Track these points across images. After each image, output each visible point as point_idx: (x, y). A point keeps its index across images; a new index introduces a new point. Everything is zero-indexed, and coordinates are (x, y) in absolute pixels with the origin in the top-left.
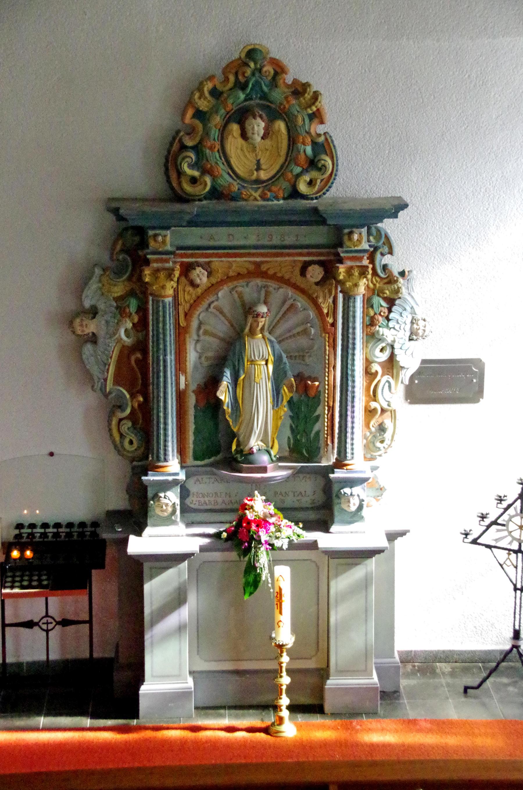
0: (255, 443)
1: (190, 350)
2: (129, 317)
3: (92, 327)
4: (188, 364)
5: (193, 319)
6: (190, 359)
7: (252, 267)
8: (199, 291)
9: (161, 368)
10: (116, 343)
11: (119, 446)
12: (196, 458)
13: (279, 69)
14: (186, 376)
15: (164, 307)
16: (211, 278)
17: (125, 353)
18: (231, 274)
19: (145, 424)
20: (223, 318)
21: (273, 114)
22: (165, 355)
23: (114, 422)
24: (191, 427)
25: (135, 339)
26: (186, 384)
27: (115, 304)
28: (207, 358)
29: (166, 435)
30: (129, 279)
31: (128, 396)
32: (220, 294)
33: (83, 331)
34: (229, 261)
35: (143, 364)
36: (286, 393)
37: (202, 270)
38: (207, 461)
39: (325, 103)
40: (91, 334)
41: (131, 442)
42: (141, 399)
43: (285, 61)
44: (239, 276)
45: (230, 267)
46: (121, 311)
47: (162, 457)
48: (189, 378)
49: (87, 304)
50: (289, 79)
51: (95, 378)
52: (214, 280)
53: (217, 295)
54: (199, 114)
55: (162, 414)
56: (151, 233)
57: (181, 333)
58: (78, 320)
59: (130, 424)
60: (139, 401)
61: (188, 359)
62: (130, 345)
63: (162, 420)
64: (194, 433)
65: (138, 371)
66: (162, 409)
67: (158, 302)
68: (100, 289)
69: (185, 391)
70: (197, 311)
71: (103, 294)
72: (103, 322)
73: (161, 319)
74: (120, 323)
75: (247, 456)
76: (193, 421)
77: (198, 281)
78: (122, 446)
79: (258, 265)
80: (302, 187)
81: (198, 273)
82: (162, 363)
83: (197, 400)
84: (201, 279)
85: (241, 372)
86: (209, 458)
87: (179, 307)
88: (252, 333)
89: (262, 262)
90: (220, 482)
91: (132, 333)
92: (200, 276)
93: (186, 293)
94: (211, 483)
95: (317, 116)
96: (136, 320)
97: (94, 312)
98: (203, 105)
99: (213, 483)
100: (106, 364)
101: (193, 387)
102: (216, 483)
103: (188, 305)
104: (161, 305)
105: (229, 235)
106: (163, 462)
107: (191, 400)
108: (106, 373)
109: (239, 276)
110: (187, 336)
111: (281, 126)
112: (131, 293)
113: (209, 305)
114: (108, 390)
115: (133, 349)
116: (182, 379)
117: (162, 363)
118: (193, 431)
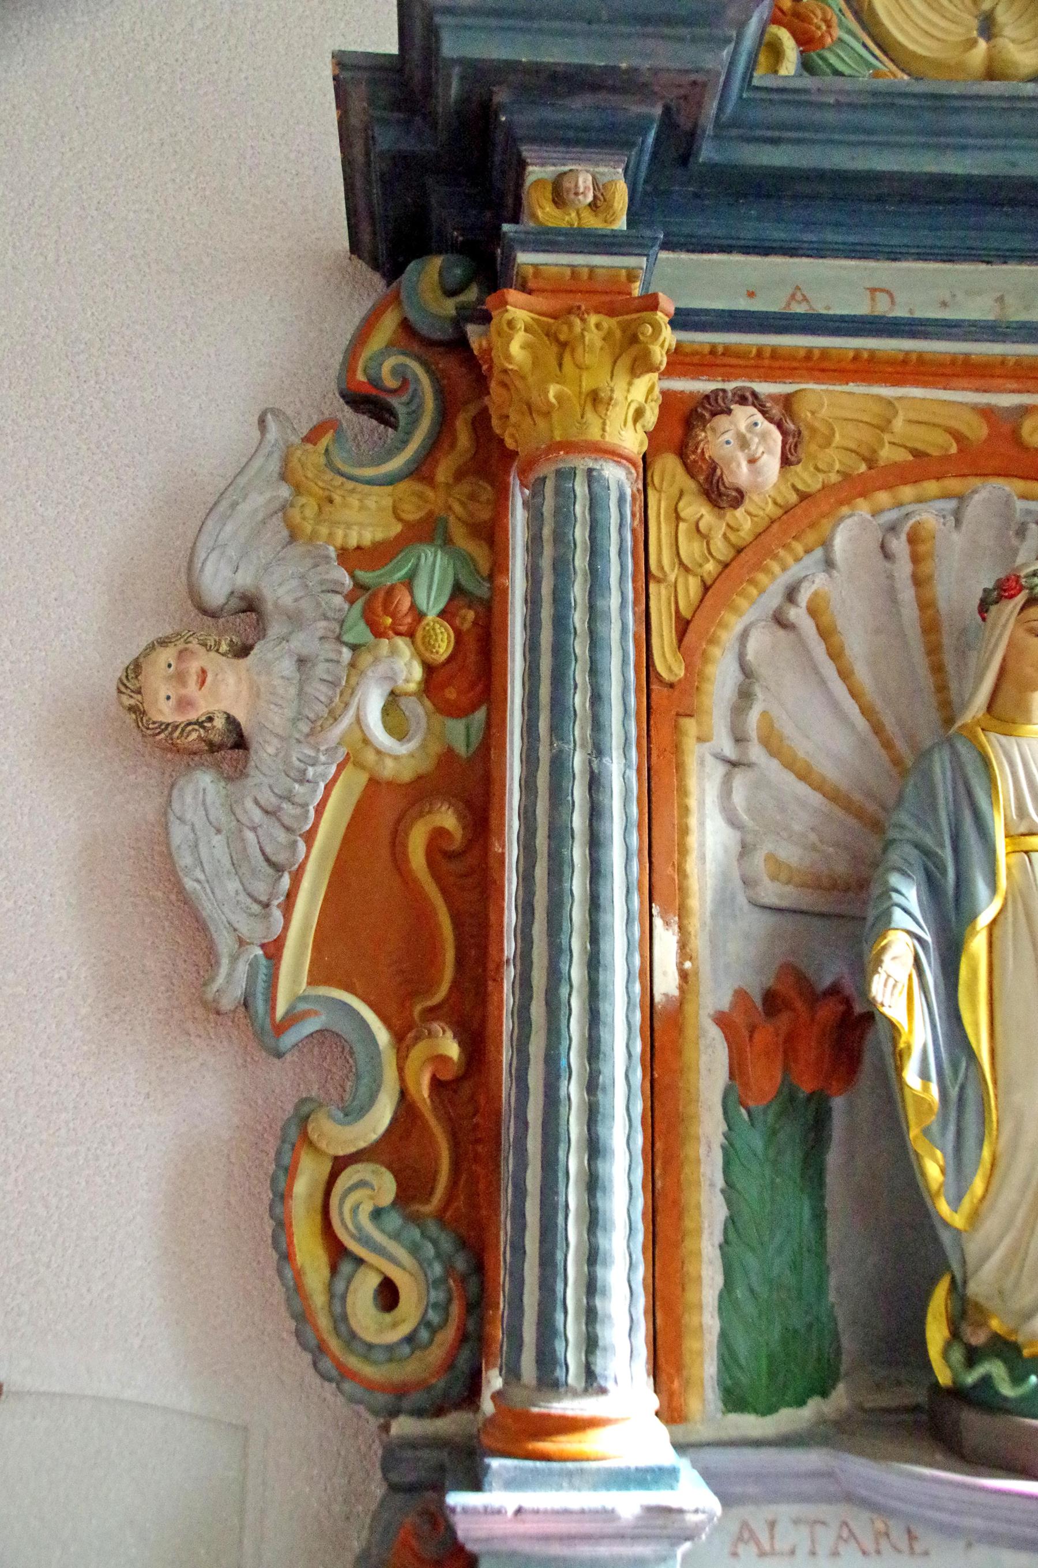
1: (702, 803)
2: (411, 634)
4: (692, 866)
5: (715, 651)
6: (702, 845)
7: (978, 431)
8: (744, 520)
9: (578, 821)
10: (341, 767)
11: (324, 1322)
12: (735, 1400)
14: (680, 928)
15: (595, 504)
16: (798, 468)
17: (381, 812)
18: (887, 454)
20: (839, 688)
22: (598, 750)
23: (305, 1185)
24: (709, 1211)
25: (435, 748)
26: (684, 975)
27: (348, 581)
28: (777, 868)
29: (593, 1220)
30: (420, 471)
31: (382, 1036)
32: (840, 541)
33: (184, 704)
34: (879, 398)
35: (469, 868)
37: (759, 417)
38: (789, 1419)
40: (219, 723)
41: (388, 1295)
42: (452, 1050)
44: (920, 466)
45: (884, 426)
46: (379, 612)
47: (573, 1358)
48: (699, 943)
49: (218, 583)
51: (225, 943)
52: (806, 478)
53: (826, 544)
55: (573, 1090)
56: (536, 173)
57: (663, 706)
58: (166, 655)
59: (386, 1186)
60: (442, 1059)
61: (692, 840)
62: (407, 775)
63: (575, 1127)
64: (725, 1246)
65: (441, 915)
66: (575, 1058)
67: (566, 475)
68: (284, 508)
69: (679, 1006)
70: (735, 610)
71: (293, 536)
72: (287, 666)
73: (580, 561)
74: (366, 659)
76: (720, 1182)
77: (740, 474)
78: (340, 1319)
81: (743, 427)
82: (579, 792)
83: (736, 1070)
84: (752, 461)
85: (981, 887)
86: (801, 1403)
87: (652, 587)
89: (1025, 411)
90: (869, 1545)
91: (417, 710)
92: (748, 447)
93: (682, 526)
94: (823, 1549)
96: (443, 646)
99: (835, 1554)
101: (714, 997)
102: (850, 1553)
103: (694, 585)
104: (581, 488)
105: (873, 290)
106: (575, 1394)
107: (709, 1064)
108: (277, 914)
109: (920, 466)
110: (690, 725)
112: (427, 530)
113: (791, 595)
114: (281, 1010)
115: (419, 793)
116: (666, 941)
117: (579, 792)
118: (718, 1238)
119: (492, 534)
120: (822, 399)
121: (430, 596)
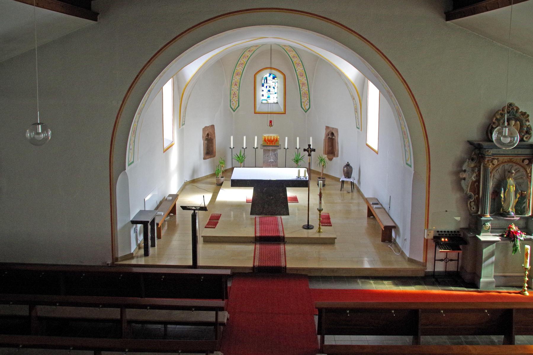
0: (510, 210)
3: (464, 175)
13: (518, 109)
17: (473, 183)
19: (479, 202)
21: (516, 120)
23: (469, 202)
36: (518, 196)
39: (530, 118)
43: (519, 107)
49: (464, 169)
50: (520, 111)
54: (497, 119)
75: (508, 213)
79: (511, 159)
80: (525, 139)
88: (509, 178)
95: (528, 121)
97: (465, 171)
98: (498, 117)
100: (468, 186)
111: (518, 122)
112: (475, 167)
115: (475, 182)
119: (480, 166)
120: (501, 159)
121: (476, 171)
